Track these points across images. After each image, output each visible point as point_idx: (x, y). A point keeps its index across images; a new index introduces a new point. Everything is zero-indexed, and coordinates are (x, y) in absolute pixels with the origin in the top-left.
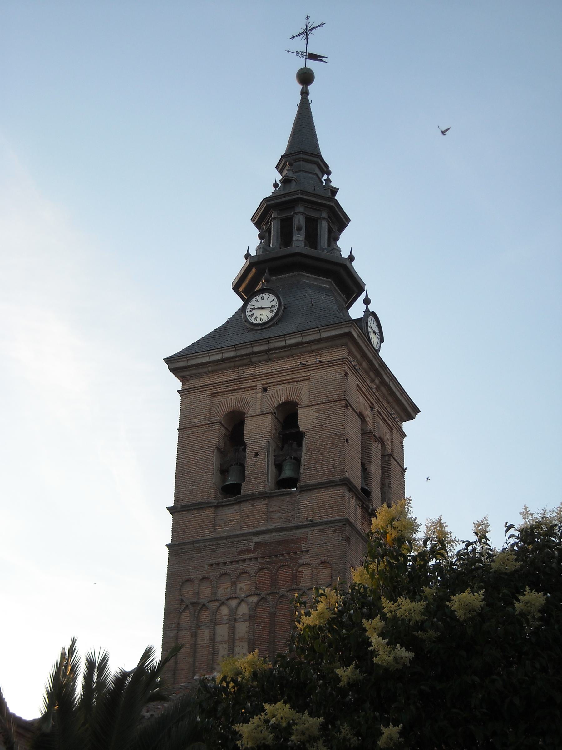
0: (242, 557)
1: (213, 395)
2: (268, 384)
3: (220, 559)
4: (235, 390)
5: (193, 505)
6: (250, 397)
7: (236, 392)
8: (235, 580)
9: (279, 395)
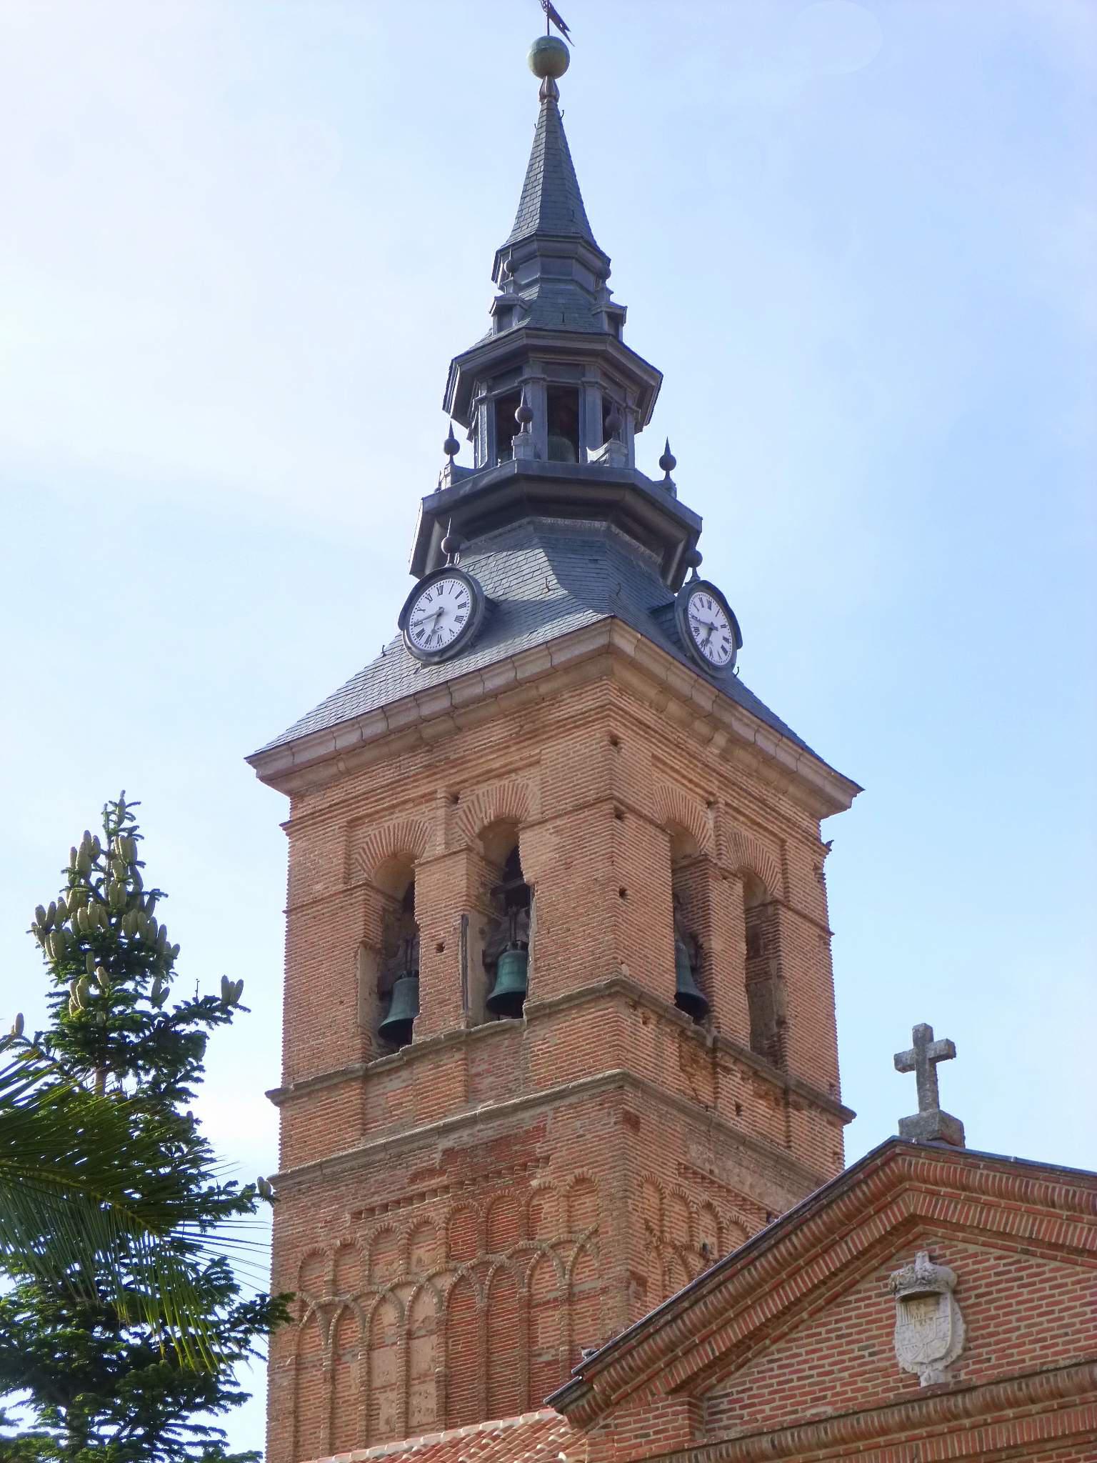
0: (421, 1186)
1: (353, 824)
2: (458, 783)
3: (376, 1198)
4: (394, 806)
5: (318, 1080)
6: (423, 820)
7: (397, 810)
8: (406, 1241)
9: (483, 806)
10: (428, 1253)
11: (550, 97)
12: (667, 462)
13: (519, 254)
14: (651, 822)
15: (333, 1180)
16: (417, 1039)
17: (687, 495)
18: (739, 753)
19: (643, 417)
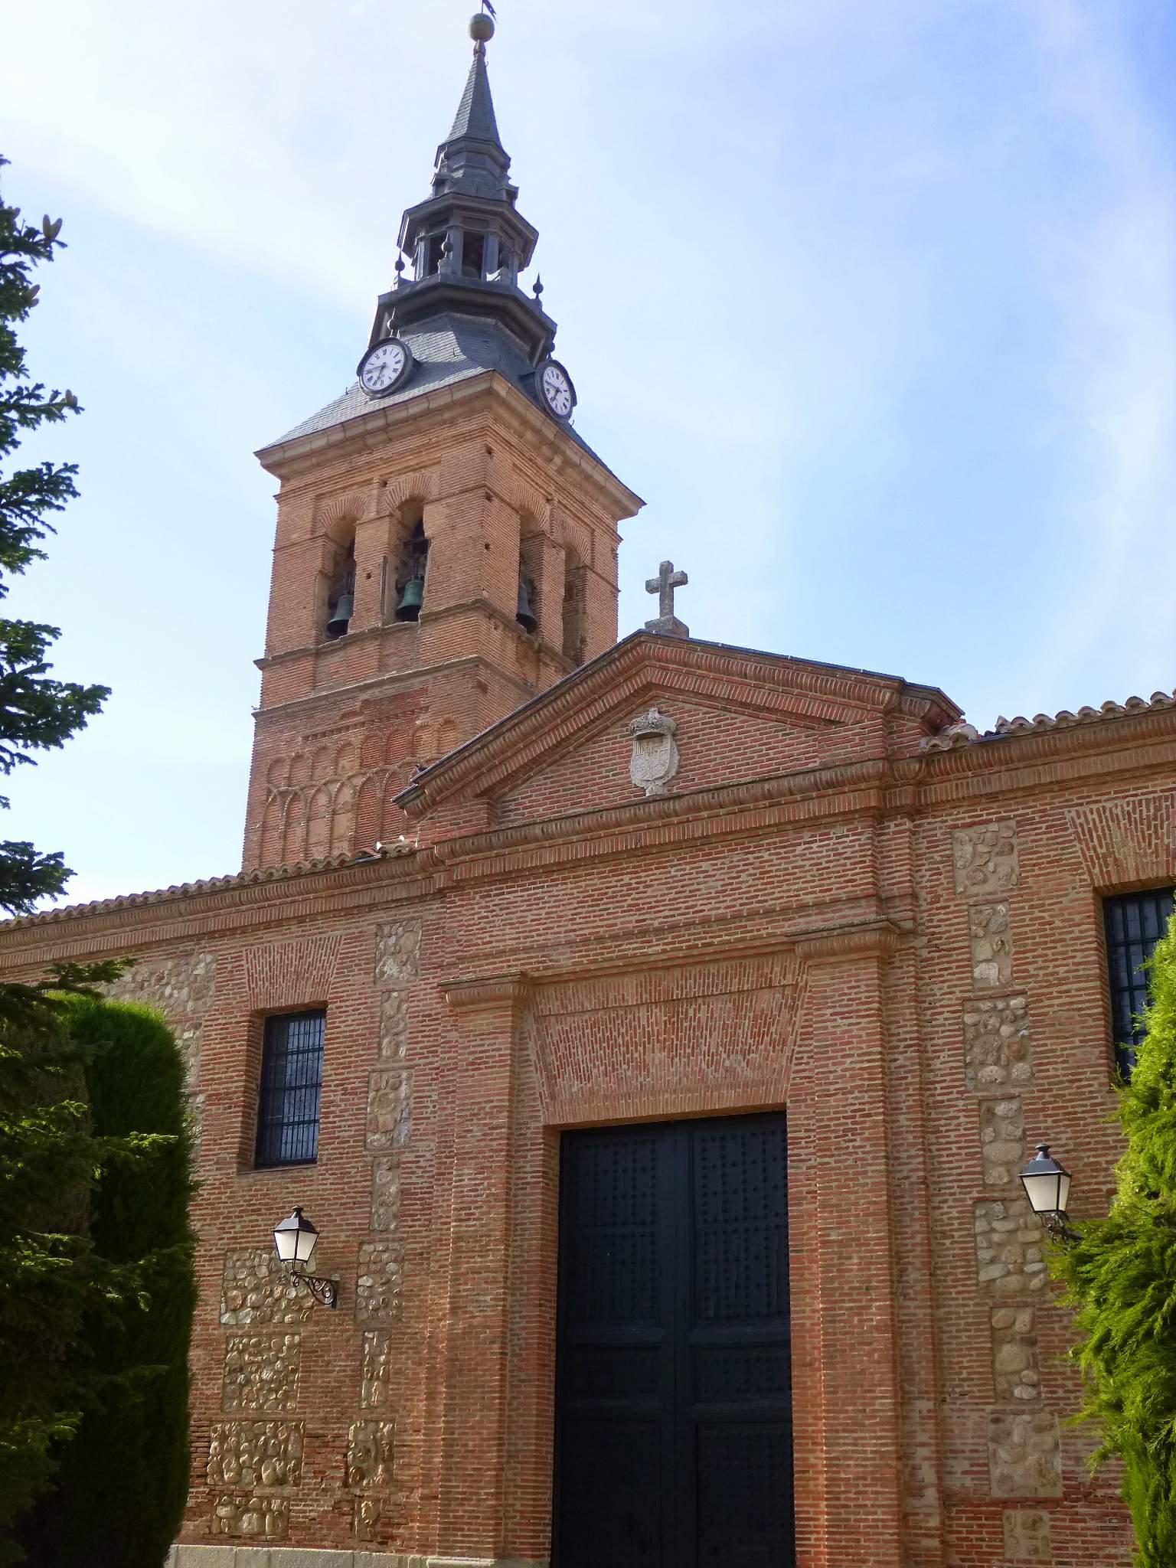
10: (349, 763)
11: (480, 53)
12: (538, 288)
13: (453, 149)
14: (509, 505)
15: (292, 716)
16: (350, 632)
17: (547, 309)
18: (569, 470)
19: (524, 263)
